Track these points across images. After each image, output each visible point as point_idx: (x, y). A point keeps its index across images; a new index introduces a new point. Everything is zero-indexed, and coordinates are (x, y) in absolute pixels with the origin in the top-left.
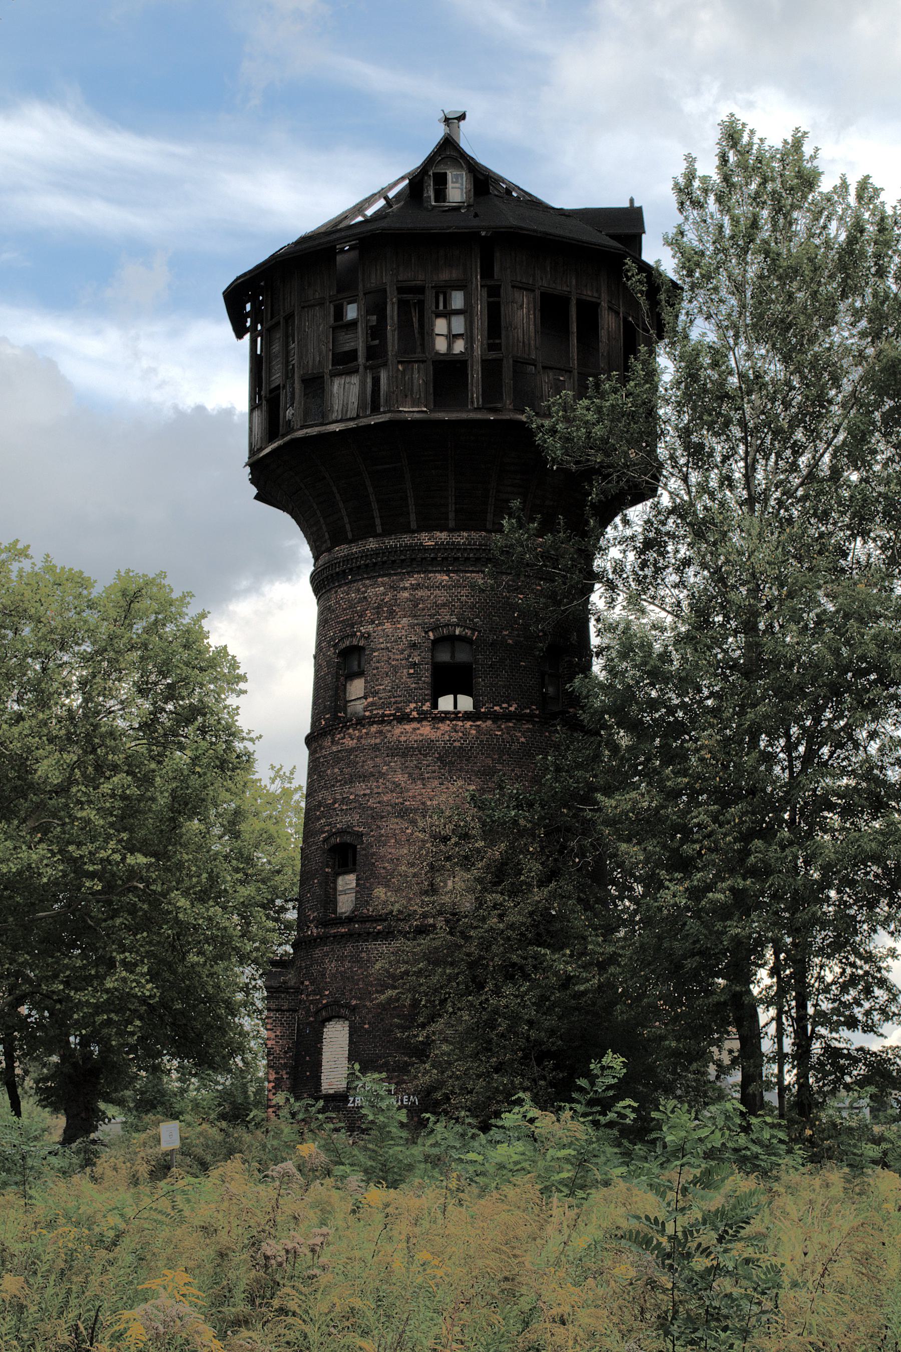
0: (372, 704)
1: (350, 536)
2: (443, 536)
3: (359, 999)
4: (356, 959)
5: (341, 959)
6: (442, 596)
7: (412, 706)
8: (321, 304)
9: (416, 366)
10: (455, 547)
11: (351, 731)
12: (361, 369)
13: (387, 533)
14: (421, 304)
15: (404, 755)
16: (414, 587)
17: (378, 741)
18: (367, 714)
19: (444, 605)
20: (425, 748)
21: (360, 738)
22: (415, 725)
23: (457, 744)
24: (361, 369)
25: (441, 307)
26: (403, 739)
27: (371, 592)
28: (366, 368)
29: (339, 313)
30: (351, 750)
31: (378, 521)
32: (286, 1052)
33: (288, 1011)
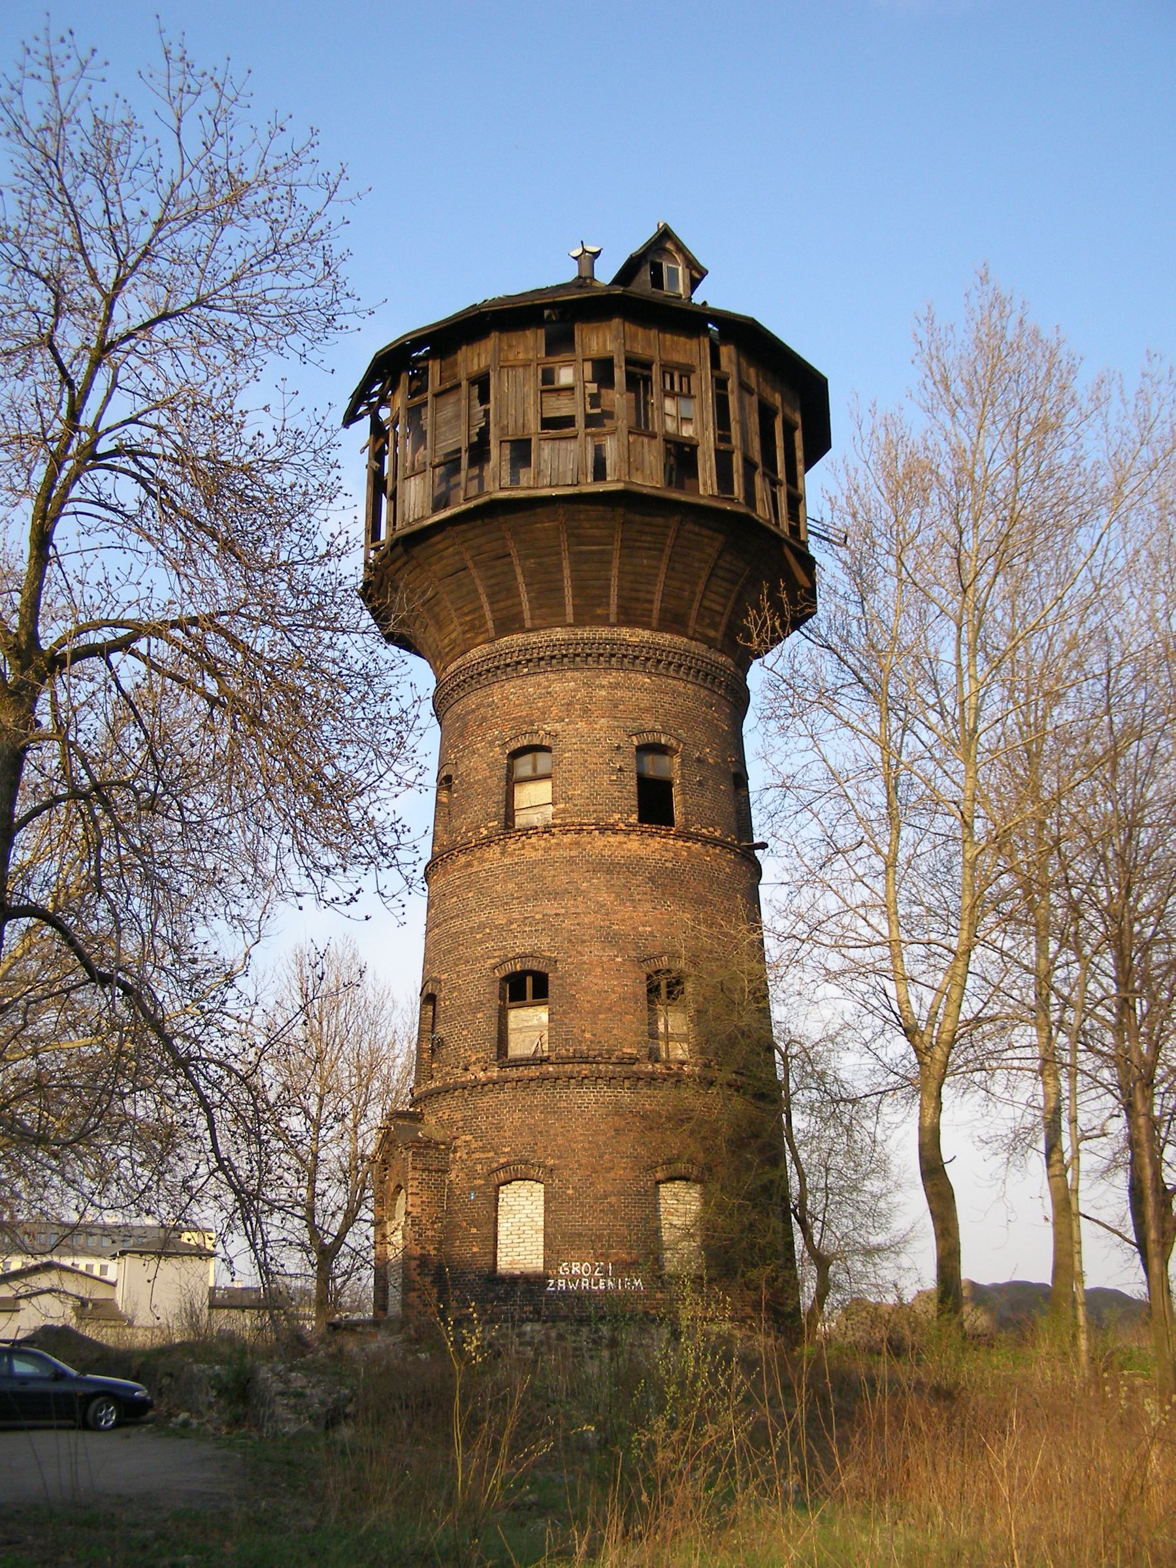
0: (564, 811)
1: (528, 624)
2: (646, 634)
3: (559, 1158)
4: (550, 1110)
5: (531, 1108)
6: (646, 700)
7: (617, 816)
8: (526, 365)
9: (646, 440)
10: (656, 647)
11: (534, 839)
12: (581, 435)
13: (579, 622)
14: (648, 380)
15: (609, 872)
16: (615, 686)
17: (573, 853)
18: (558, 821)
19: (647, 710)
20: (633, 866)
21: (546, 850)
22: (621, 838)
23: (669, 865)
24: (581, 435)
25: (668, 387)
26: (606, 852)
27: (557, 687)
28: (587, 435)
29: (548, 377)
30: (536, 863)
31: (569, 609)
32: (433, 1223)
33: (437, 1171)
